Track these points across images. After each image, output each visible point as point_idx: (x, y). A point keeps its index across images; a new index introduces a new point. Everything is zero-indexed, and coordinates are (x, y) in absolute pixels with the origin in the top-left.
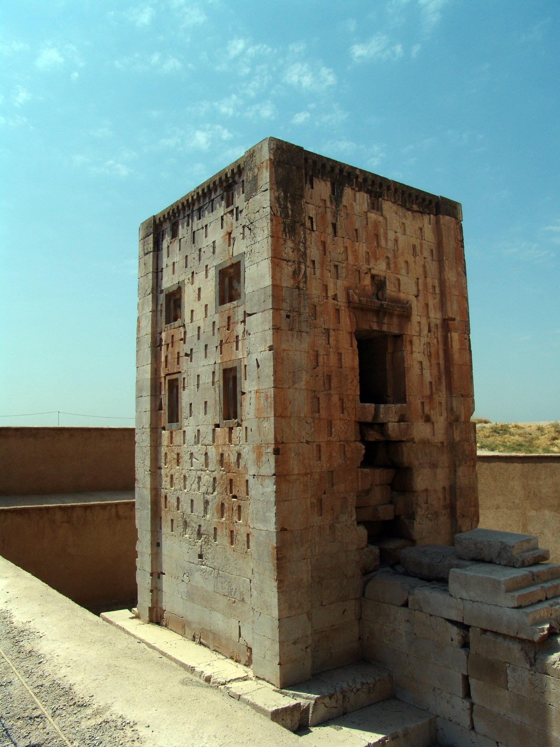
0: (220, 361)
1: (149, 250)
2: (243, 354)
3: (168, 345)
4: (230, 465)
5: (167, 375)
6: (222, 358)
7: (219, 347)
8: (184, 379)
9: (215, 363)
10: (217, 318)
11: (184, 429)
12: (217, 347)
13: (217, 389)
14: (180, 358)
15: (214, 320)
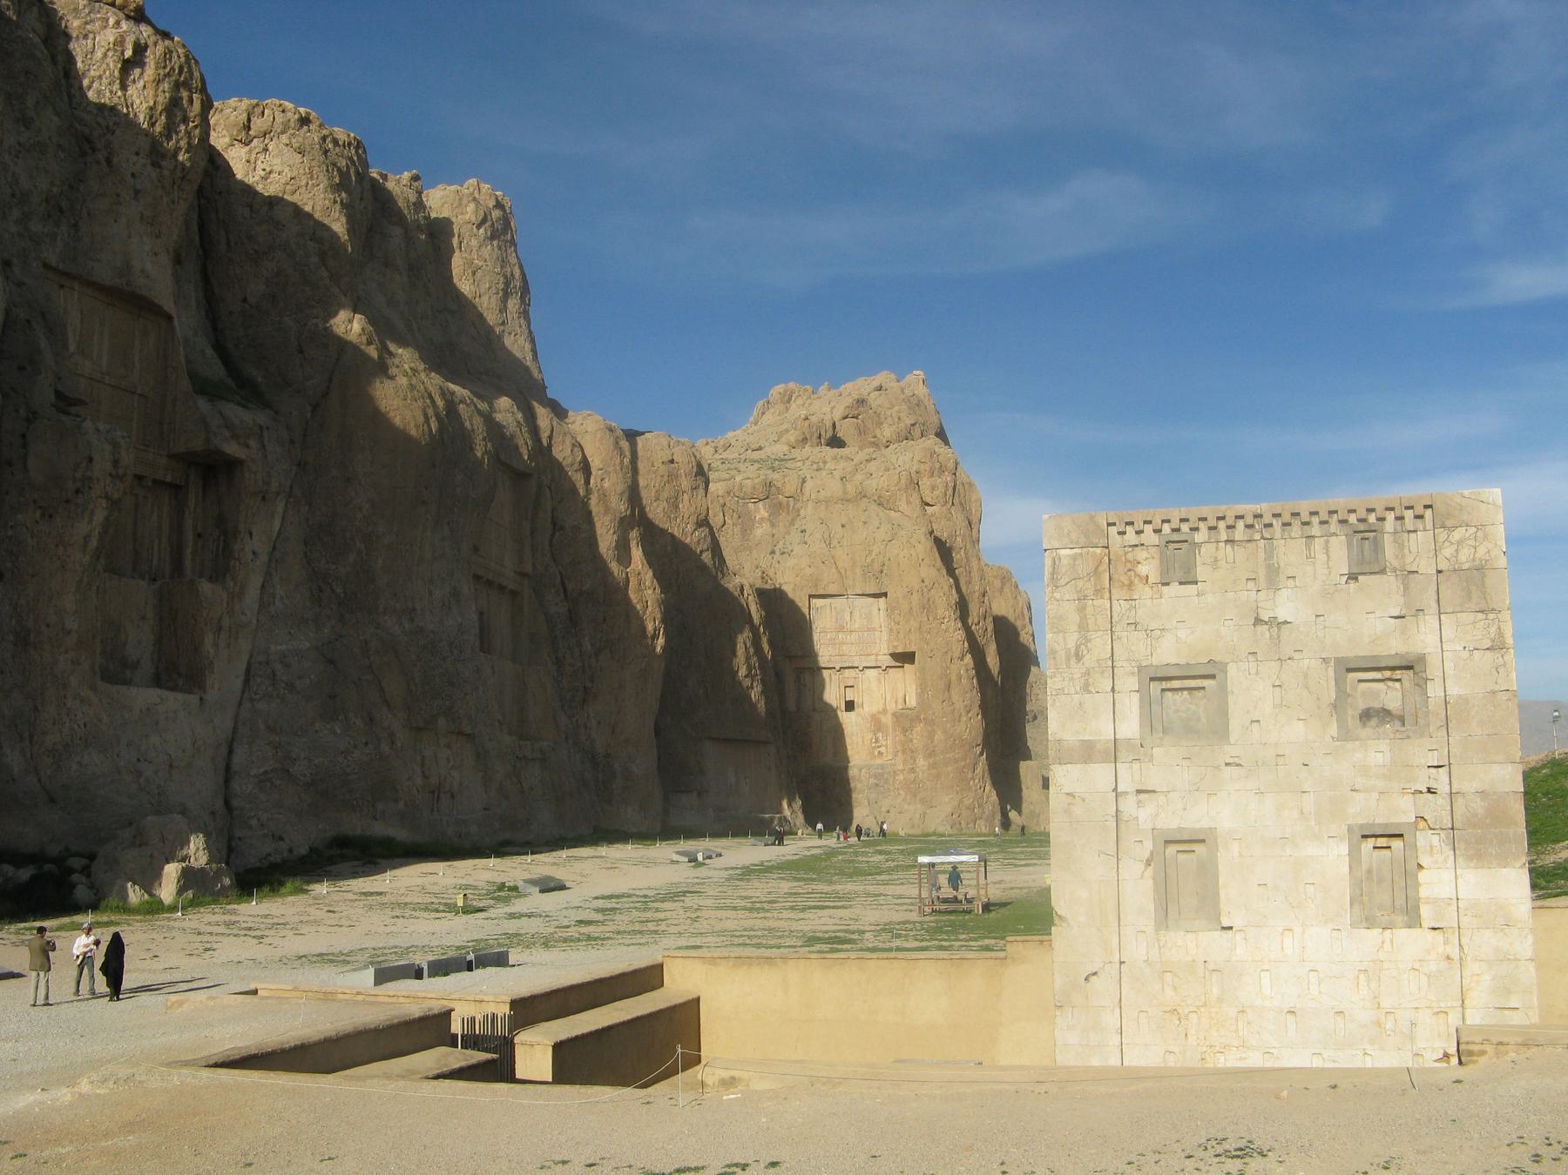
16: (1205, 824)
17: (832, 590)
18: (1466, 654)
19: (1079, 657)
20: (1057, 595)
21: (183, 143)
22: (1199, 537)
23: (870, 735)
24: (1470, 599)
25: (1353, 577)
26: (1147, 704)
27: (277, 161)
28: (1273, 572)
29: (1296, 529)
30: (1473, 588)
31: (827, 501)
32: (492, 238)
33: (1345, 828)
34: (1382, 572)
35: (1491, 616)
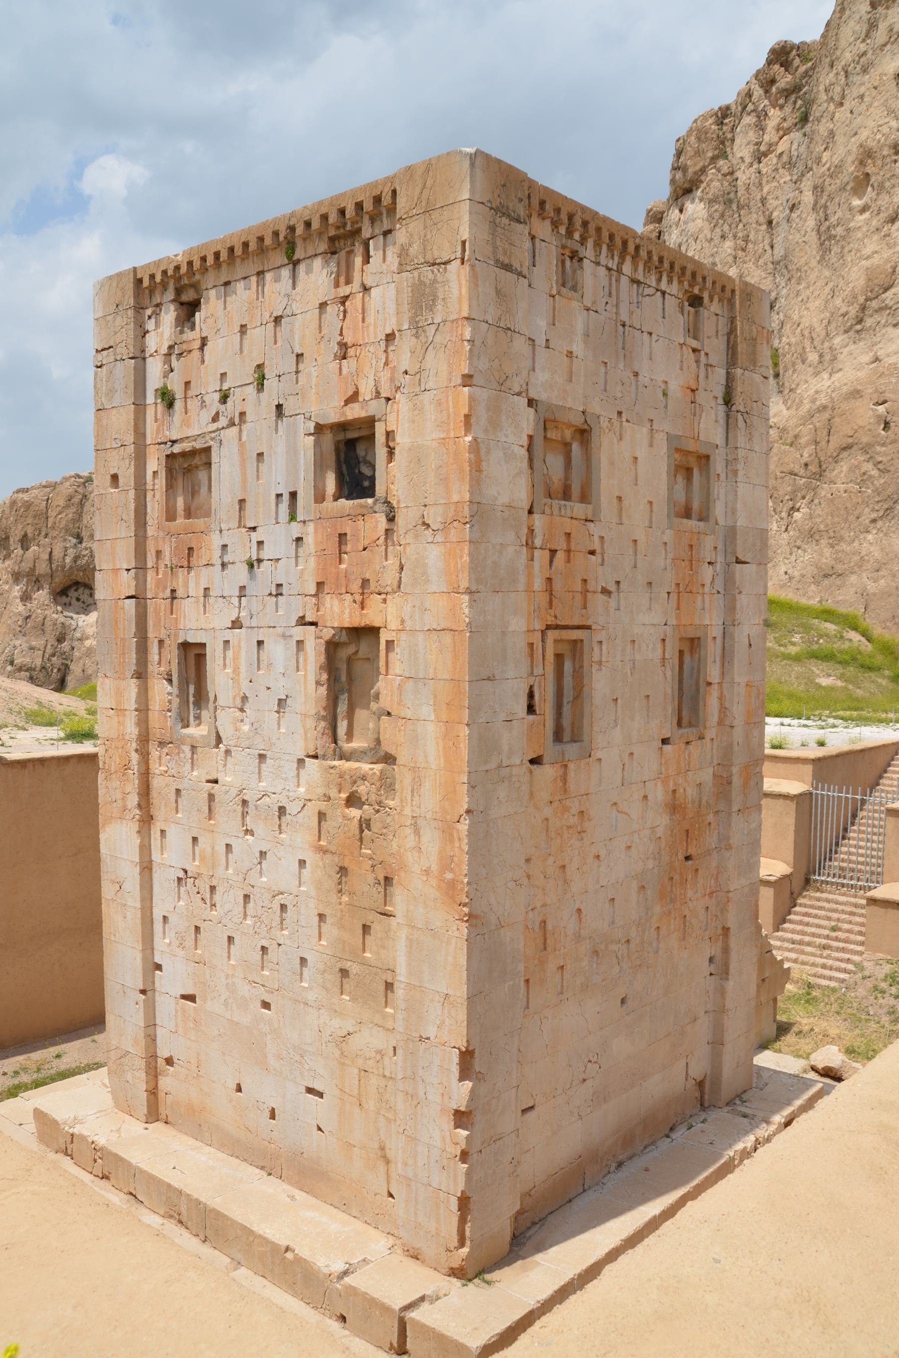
0: (674, 623)
1: (516, 265)
2: (711, 619)
3: (553, 552)
4: (686, 807)
5: (548, 627)
6: (678, 617)
7: (674, 596)
8: (601, 642)
9: (665, 624)
10: (668, 536)
11: (599, 754)
12: (668, 593)
13: (669, 673)
14: (589, 595)
15: (665, 539)
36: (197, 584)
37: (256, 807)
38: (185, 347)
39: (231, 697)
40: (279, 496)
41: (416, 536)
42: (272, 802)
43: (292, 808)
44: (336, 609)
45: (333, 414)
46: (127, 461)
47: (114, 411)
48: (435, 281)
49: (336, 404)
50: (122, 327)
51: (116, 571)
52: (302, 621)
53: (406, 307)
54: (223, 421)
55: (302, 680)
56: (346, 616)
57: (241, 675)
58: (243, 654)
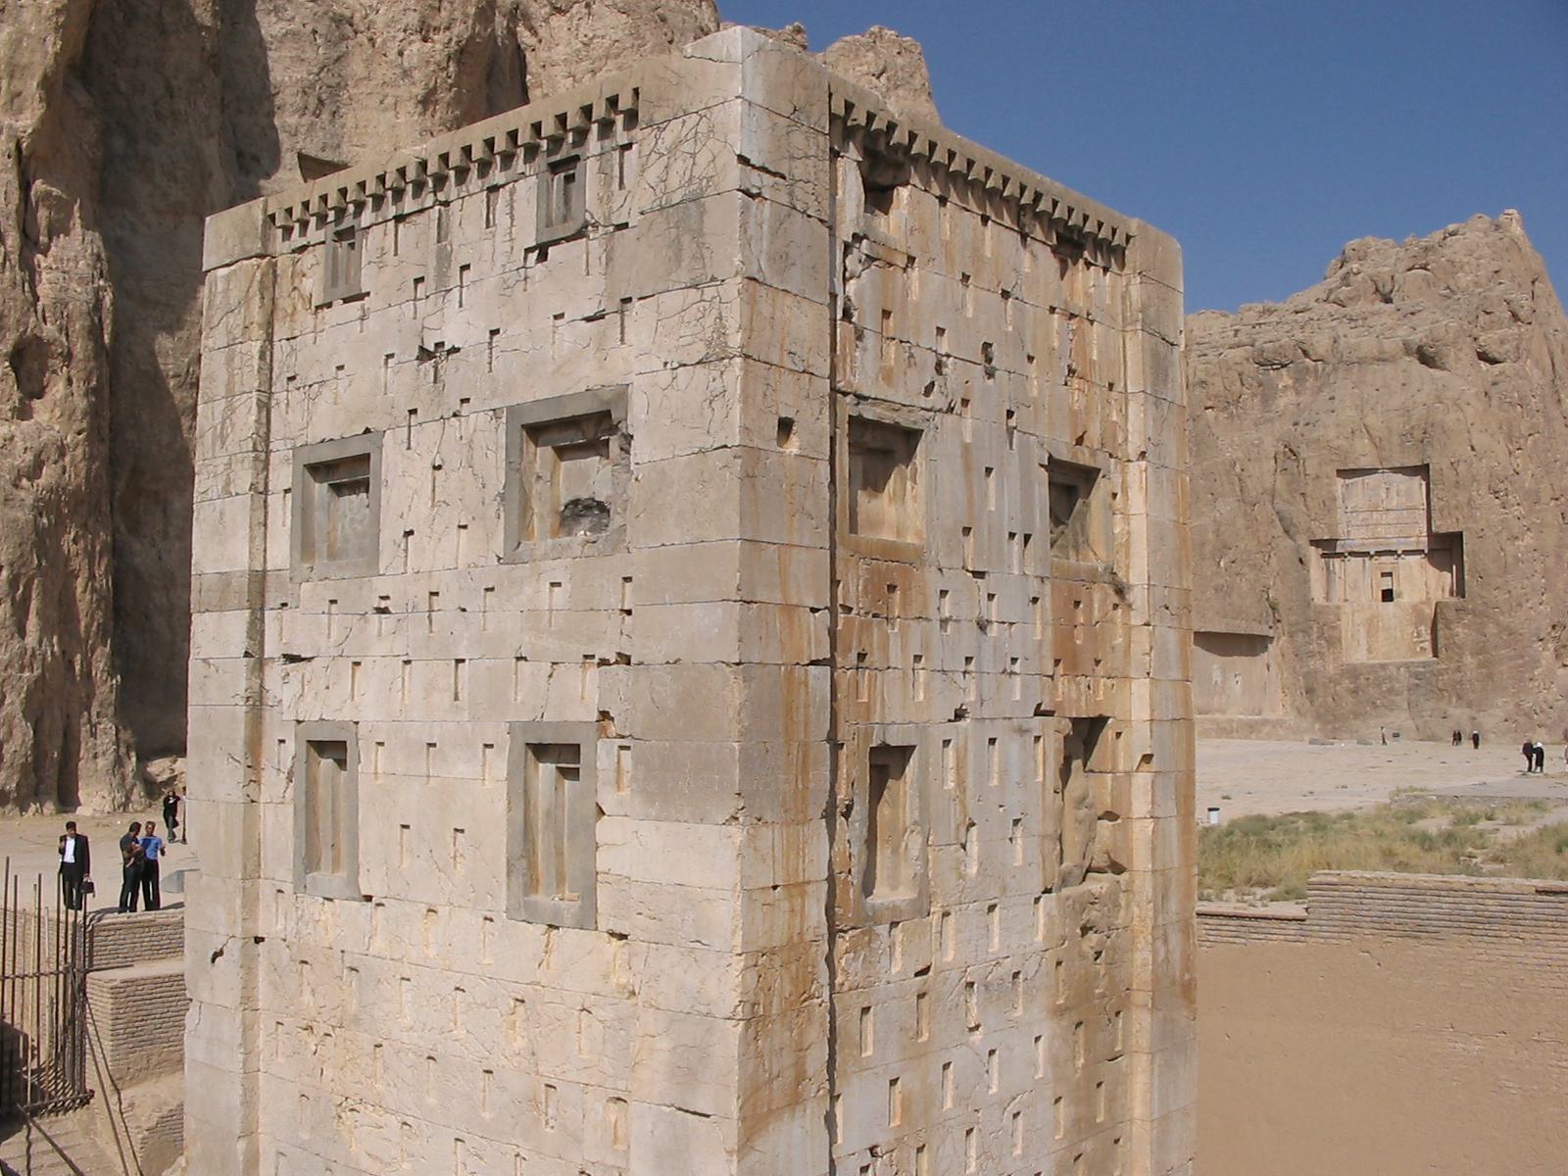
16: (347, 715)
17: (1364, 463)
18: (665, 377)
19: (223, 439)
20: (210, 343)
21: (457, 14)
22: (367, 217)
23: (1410, 629)
24: (679, 260)
25: (542, 251)
26: (304, 515)
27: (598, 25)
28: (444, 258)
29: (474, 182)
30: (686, 239)
31: (1361, 362)
32: (897, 87)
33: (505, 727)
34: (580, 234)
35: (709, 293)
36: (904, 648)
37: (986, 987)
38: (881, 252)
39: (953, 826)
40: (1012, 535)
41: (1162, 619)
42: (1008, 967)
43: (1029, 969)
44: (1074, 695)
45: (1066, 452)
46: (816, 405)
47: (789, 300)
48: (1166, 357)
49: (1068, 440)
50: (807, 157)
51: (789, 609)
52: (1038, 712)
53: (1148, 369)
54: (936, 400)
55: (1040, 788)
56: (1083, 704)
57: (968, 792)
58: (971, 756)
